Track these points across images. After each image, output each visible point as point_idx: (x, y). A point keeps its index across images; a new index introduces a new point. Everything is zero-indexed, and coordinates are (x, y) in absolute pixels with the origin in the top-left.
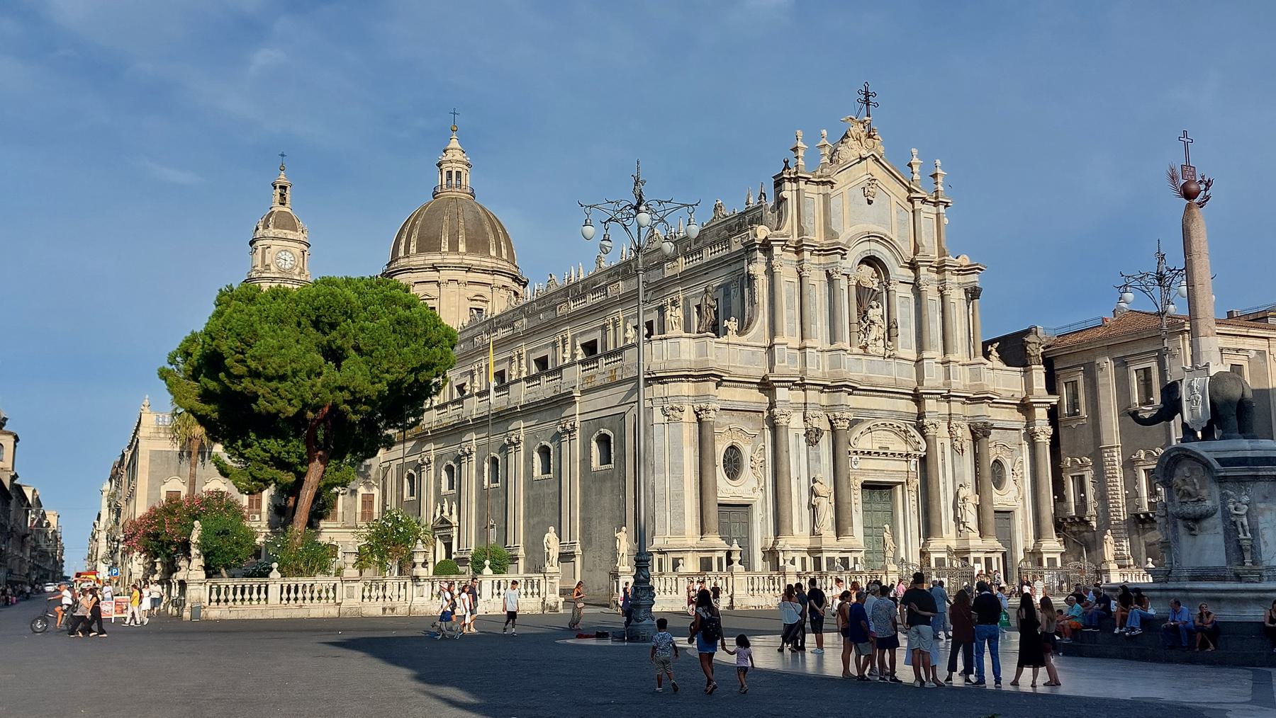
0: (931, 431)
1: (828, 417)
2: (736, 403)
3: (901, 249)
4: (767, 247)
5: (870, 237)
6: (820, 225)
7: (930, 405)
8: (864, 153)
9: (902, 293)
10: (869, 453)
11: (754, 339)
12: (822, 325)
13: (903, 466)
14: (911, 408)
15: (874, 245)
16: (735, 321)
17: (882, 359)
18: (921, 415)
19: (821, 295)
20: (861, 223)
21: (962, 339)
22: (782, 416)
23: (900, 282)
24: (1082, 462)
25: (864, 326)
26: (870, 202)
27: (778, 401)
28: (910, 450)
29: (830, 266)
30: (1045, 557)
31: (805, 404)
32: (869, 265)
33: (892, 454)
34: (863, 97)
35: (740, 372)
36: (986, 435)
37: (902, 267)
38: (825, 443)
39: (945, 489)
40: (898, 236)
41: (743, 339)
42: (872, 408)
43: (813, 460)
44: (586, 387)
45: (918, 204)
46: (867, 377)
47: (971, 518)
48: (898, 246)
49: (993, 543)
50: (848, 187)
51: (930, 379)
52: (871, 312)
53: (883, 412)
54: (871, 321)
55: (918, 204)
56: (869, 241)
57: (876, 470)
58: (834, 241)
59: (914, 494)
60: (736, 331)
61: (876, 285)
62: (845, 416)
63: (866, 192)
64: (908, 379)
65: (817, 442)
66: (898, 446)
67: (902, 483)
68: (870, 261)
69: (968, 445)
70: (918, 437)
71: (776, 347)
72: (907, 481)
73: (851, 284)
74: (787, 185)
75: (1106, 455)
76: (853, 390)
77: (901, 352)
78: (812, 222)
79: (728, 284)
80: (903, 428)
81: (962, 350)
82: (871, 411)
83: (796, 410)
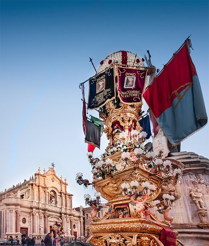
7: (63, 215)
14: (59, 215)
15: (53, 189)
26: (53, 182)
31: (39, 212)
35: (26, 205)
45: (62, 184)
52: (53, 199)
55: (62, 184)
62: (47, 215)
70: (61, 220)
76: (49, 211)
77: (58, 206)
83: (37, 213)
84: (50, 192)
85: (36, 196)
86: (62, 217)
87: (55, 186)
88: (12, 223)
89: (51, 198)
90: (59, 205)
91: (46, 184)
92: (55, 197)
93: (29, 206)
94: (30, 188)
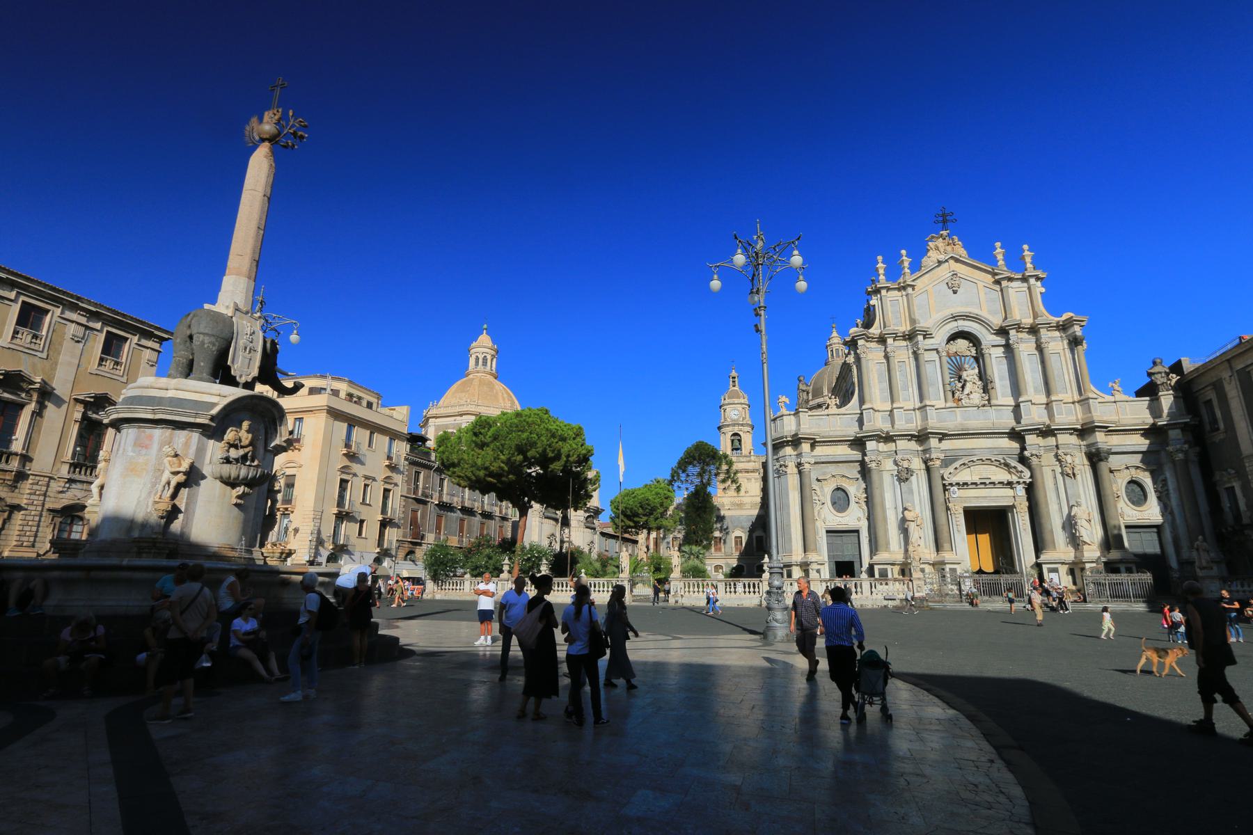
0: (1034, 461)
5: (955, 318)
7: (1031, 439)
8: (942, 257)
10: (965, 484)
13: (1009, 492)
15: (961, 323)
16: (835, 398)
17: (976, 408)
18: (1023, 449)
21: (1070, 381)
23: (993, 346)
25: (960, 385)
26: (955, 292)
28: (1014, 479)
33: (990, 483)
34: (941, 219)
37: (992, 334)
38: (919, 482)
41: (843, 410)
42: (970, 447)
45: (1004, 283)
50: (931, 286)
51: (1027, 419)
54: (965, 381)
55: (1004, 283)
56: (956, 320)
60: (836, 404)
63: (950, 285)
64: (1008, 422)
65: (907, 479)
66: (1002, 475)
70: (1020, 467)
80: (1002, 461)
85: (880, 382)
86: (1027, 453)
87: (974, 310)
90: (1003, 394)
91: (917, 316)
92: (979, 358)
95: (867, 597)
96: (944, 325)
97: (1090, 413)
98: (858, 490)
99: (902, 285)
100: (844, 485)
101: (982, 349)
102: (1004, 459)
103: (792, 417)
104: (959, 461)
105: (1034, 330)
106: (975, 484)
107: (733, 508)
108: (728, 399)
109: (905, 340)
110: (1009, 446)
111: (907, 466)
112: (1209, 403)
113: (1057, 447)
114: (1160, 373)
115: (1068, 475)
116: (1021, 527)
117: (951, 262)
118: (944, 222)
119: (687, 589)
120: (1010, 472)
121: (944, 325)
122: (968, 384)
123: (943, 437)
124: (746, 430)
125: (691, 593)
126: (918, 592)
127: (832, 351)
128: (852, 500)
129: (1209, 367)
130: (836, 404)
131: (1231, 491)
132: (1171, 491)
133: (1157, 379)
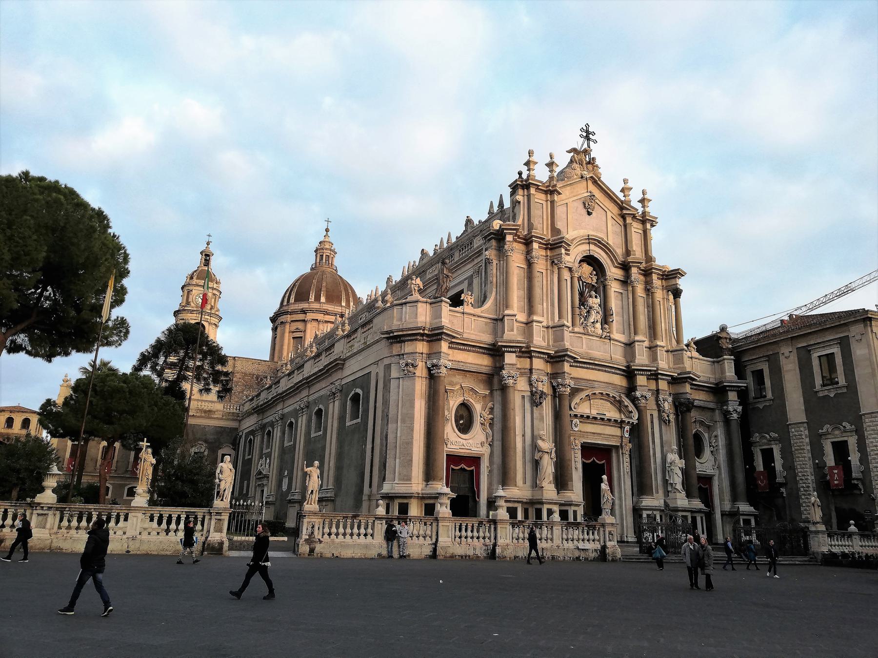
1: (552, 383)
2: (469, 365)
3: (616, 252)
4: (500, 236)
5: (590, 240)
6: (547, 224)
7: (641, 380)
9: (614, 288)
10: (588, 417)
11: (487, 311)
12: (547, 305)
13: (617, 431)
15: (592, 247)
16: (471, 295)
19: (547, 281)
20: (583, 229)
21: (666, 330)
22: (509, 378)
23: (615, 279)
24: (770, 437)
26: (589, 214)
27: (506, 364)
29: (555, 257)
30: (742, 518)
31: (531, 370)
32: (589, 264)
34: (585, 134)
35: (473, 337)
36: (689, 410)
37: (616, 267)
38: (547, 407)
39: (654, 454)
40: (613, 244)
41: (478, 311)
42: (591, 379)
43: (537, 419)
44: (348, 354)
46: (587, 353)
47: (677, 479)
48: (613, 250)
49: (697, 504)
53: (600, 384)
54: (591, 308)
55: (629, 220)
57: (594, 433)
58: (560, 236)
59: (627, 456)
60: (471, 303)
61: (595, 281)
62: (567, 381)
63: (587, 205)
65: (541, 403)
66: (612, 413)
67: (617, 447)
68: (590, 260)
69: (672, 417)
70: (631, 407)
71: (506, 318)
72: (621, 444)
73: (573, 276)
74: (520, 191)
75: (793, 430)
78: (541, 222)
79: (472, 276)
80: (618, 398)
81: (666, 340)
82: (590, 382)
83: (522, 374)
84: (577, 265)
85: (518, 289)
86: (638, 394)
87: (601, 235)
88: (412, 430)
89: (581, 294)
91: (559, 225)
92: (601, 288)
93: (486, 338)
94: (490, 254)
95: (558, 547)
96: (579, 245)
97: (683, 364)
98: (484, 409)
99: (551, 188)
100: (471, 400)
101: (606, 280)
102: (620, 397)
103: (428, 305)
104: (584, 392)
105: (647, 273)
106: (595, 418)
107: (198, 415)
108: (197, 278)
109: (546, 249)
110: (620, 384)
111: (541, 389)
112: (759, 375)
113: (658, 391)
114: (726, 338)
115: (664, 422)
116: (625, 470)
117: (590, 183)
118: (587, 138)
119: (327, 530)
120: (620, 411)
121: (579, 245)
122: (593, 313)
123: (576, 362)
124: (214, 322)
125: (333, 536)
126: (610, 540)
127: (322, 256)
128: (477, 420)
129: (770, 341)
130: (471, 303)
131: (768, 455)
132: (720, 447)
133: (723, 343)
